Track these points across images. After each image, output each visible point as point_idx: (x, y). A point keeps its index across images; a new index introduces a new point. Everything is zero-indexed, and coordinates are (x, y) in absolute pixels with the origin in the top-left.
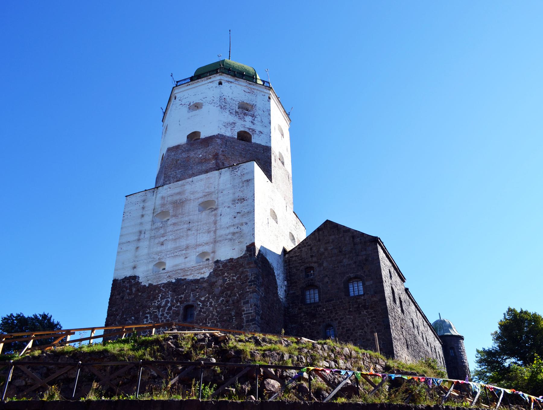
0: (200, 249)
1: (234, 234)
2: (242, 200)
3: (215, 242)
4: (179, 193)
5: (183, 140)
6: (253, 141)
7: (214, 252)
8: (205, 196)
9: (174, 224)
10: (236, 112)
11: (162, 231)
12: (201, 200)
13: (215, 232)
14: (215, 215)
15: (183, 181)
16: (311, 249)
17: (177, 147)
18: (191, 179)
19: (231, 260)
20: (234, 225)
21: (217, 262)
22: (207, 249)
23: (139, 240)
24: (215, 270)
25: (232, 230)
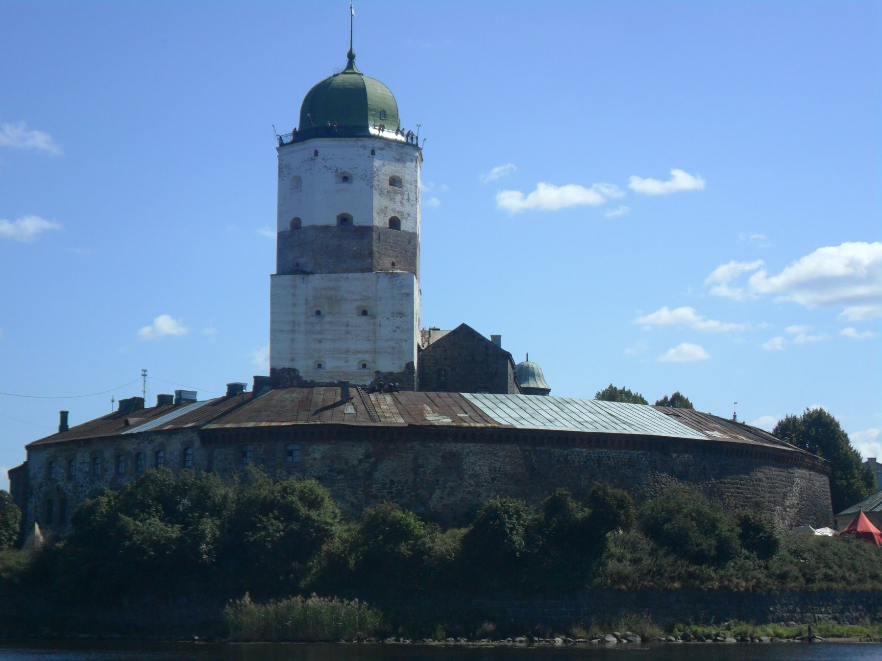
0: (361, 356)
1: (393, 348)
2: (401, 314)
3: (375, 352)
4: (332, 289)
5: (333, 222)
6: (402, 228)
7: (374, 362)
8: (363, 299)
9: (331, 323)
10: (388, 192)
11: (318, 328)
12: (358, 303)
13: (375, 341)
14: (374, 324)
15: (337, 275)
16: (445, 351)
17: (326, 228)
18: (345, 275)
19: (391, 373)
20: (393, 340)
21: (378, 372)
22: (368, 357)
23: (293, 331)
24: (376, 380)
25: (391, 343)
